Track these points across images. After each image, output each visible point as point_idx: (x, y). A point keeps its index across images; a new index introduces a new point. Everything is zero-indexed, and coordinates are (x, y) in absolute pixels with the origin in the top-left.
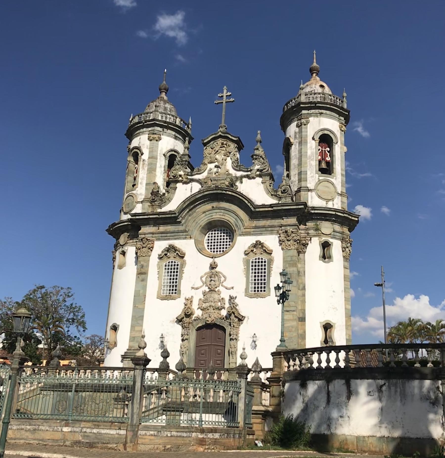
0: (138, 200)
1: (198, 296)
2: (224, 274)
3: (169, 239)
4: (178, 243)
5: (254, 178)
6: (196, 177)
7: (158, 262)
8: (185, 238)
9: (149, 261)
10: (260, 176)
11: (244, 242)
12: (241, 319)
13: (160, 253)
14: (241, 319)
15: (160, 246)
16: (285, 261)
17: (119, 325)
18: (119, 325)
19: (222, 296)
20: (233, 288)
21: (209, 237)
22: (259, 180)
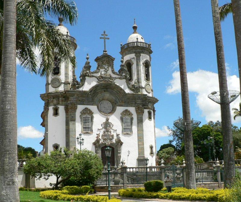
0: (62, 82)
1: (101, 133)
2: (112, 124)
3: (84, 105)
4: (90, 107)
5: (121, 79)
6: (95, 75)
7: (80, 116)
8: (92, 105)
9: (75, 114)
10: (125, 79)
11: (120, 109)
12: (122, 143)
13: (81, 110)
14: (122, 143)
15: (80, 107)
16: (138, 120)
17: (59, 145)
18: (59, 145)
19: (112, 133)
20: (116, 130)
21: (100, 105)
22: (124, 80)
